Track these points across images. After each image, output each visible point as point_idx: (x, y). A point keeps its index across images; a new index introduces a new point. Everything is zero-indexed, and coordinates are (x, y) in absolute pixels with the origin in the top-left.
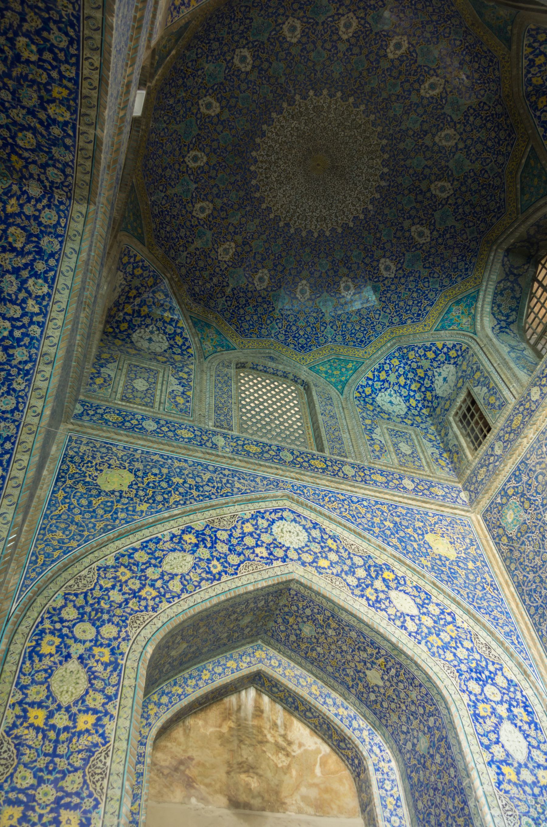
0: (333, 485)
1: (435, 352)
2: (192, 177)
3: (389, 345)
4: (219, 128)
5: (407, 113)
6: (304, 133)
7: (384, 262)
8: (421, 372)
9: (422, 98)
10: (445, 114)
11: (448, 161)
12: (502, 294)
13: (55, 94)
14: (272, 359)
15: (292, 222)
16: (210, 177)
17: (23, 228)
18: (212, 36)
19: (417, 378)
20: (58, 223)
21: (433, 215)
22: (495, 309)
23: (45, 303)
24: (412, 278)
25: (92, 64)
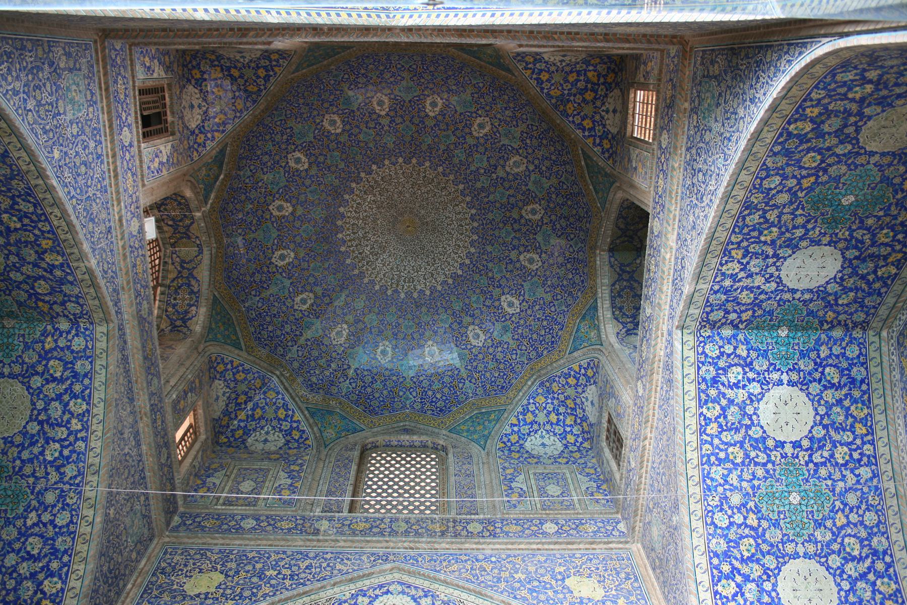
0: (454, 546)
1: (575, 377)
2: (284, 275)
3: (529, 383)
4: (297, 224)
5: (470, 155)
7: (505, 300)
10: (504, 145)
11: (527, 185)
12: (620, 296)
14: (406, 431)
15: (400, 287)
16: (303, 269)
17: (60, 359)
19: (569, 411)
21: (535, 239)
24: (537, 307)
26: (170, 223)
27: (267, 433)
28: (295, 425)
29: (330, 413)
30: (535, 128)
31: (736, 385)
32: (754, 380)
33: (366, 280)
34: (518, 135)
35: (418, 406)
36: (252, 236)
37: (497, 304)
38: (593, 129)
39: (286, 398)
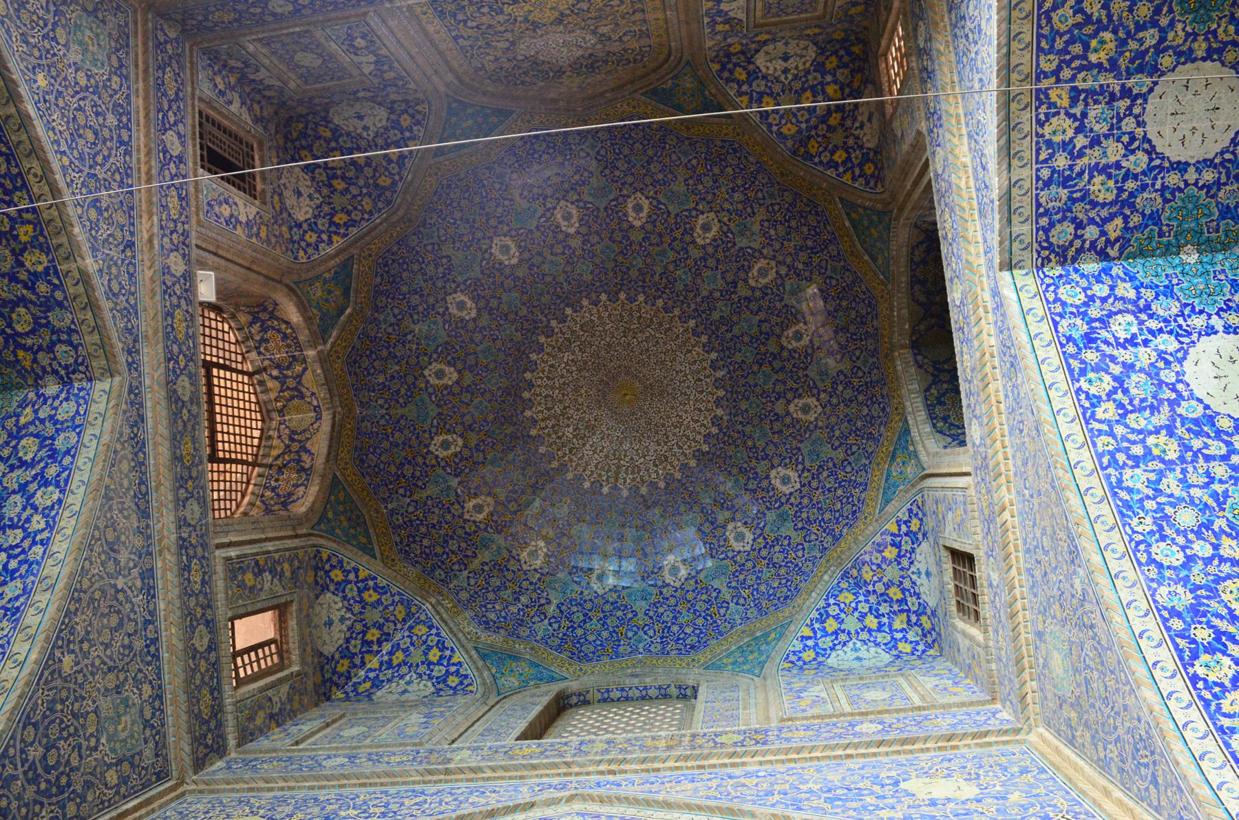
4: (466, 397)
5: (698, 274)
6: (585, 363)
8: (895, 593)
9: (704, 247)
10: (741, 249)
11: (782, 300)
12: (940, 403)
13: (24, 239)
18: (404, 289)
19: (896, 607)
20: (77, 412)
21: (807, 376)
22: (940, 424)
23: (53, 513)
24: (825, 474)
25: (35, 175)
26: (275, 373)
27: (408, 683)
28: (453, 669)
29: (515, 658)
30: (776, 208)
31: (1131, 341)
32: (1161, 331)
33: (570, 476)
34: (756, 228)
35: (656, 648)
36: (401, 411)
37: (765, 484)
38: (849, 159)
39: (443, 634)
